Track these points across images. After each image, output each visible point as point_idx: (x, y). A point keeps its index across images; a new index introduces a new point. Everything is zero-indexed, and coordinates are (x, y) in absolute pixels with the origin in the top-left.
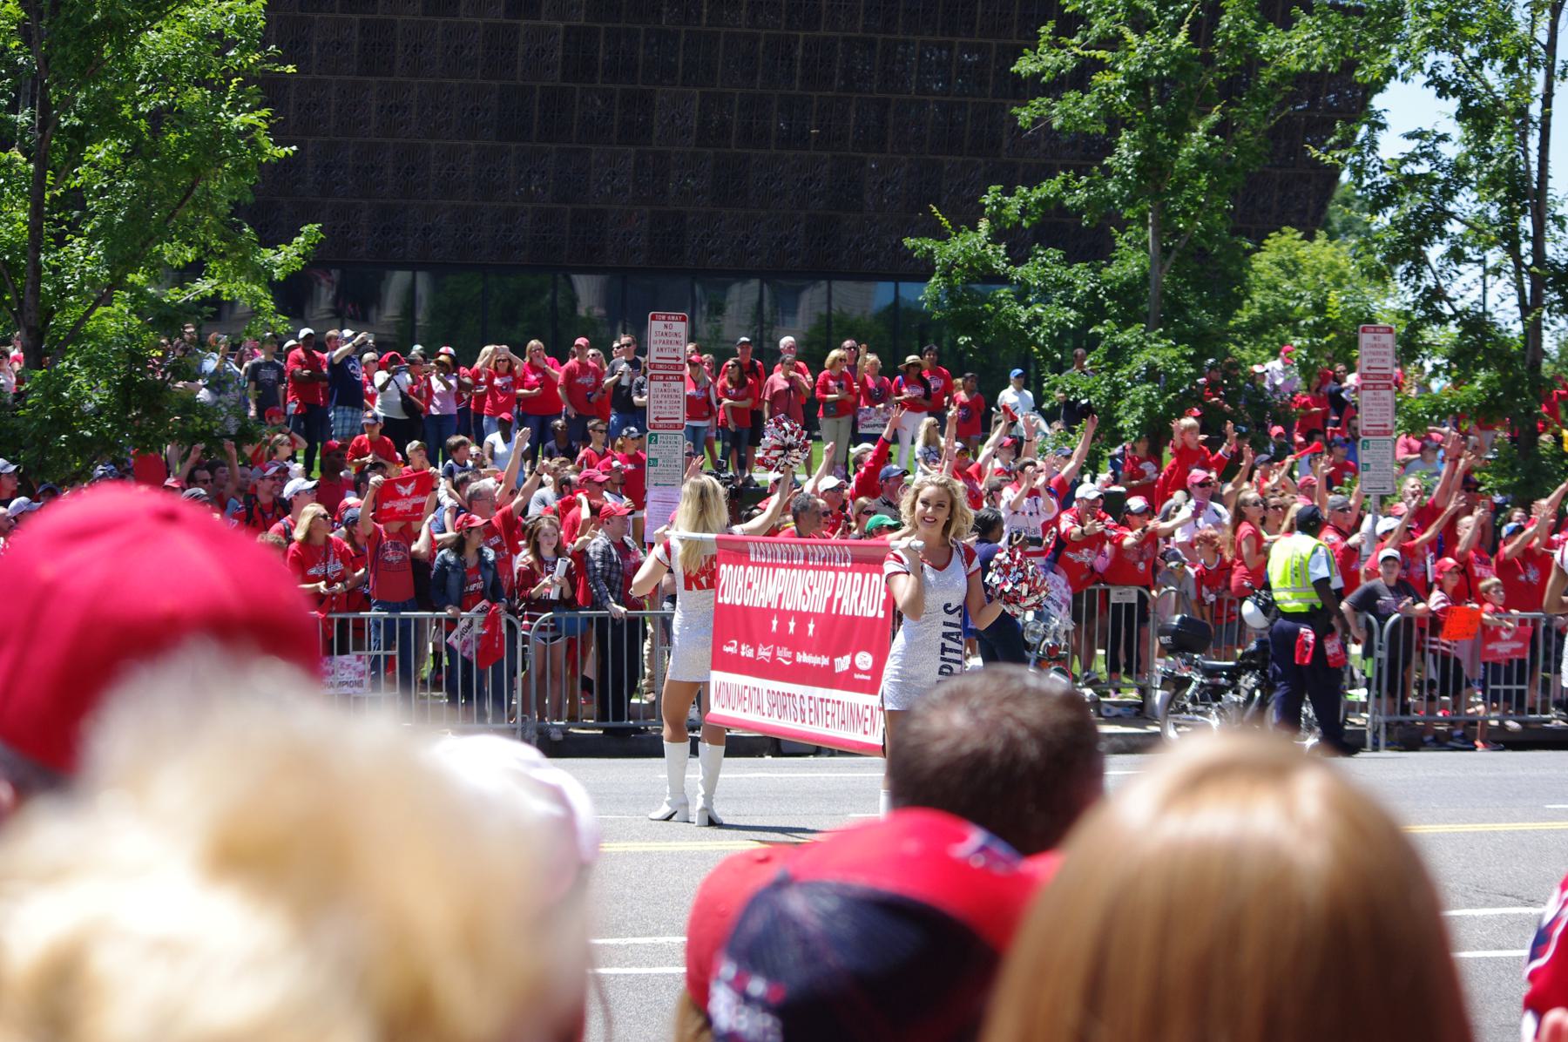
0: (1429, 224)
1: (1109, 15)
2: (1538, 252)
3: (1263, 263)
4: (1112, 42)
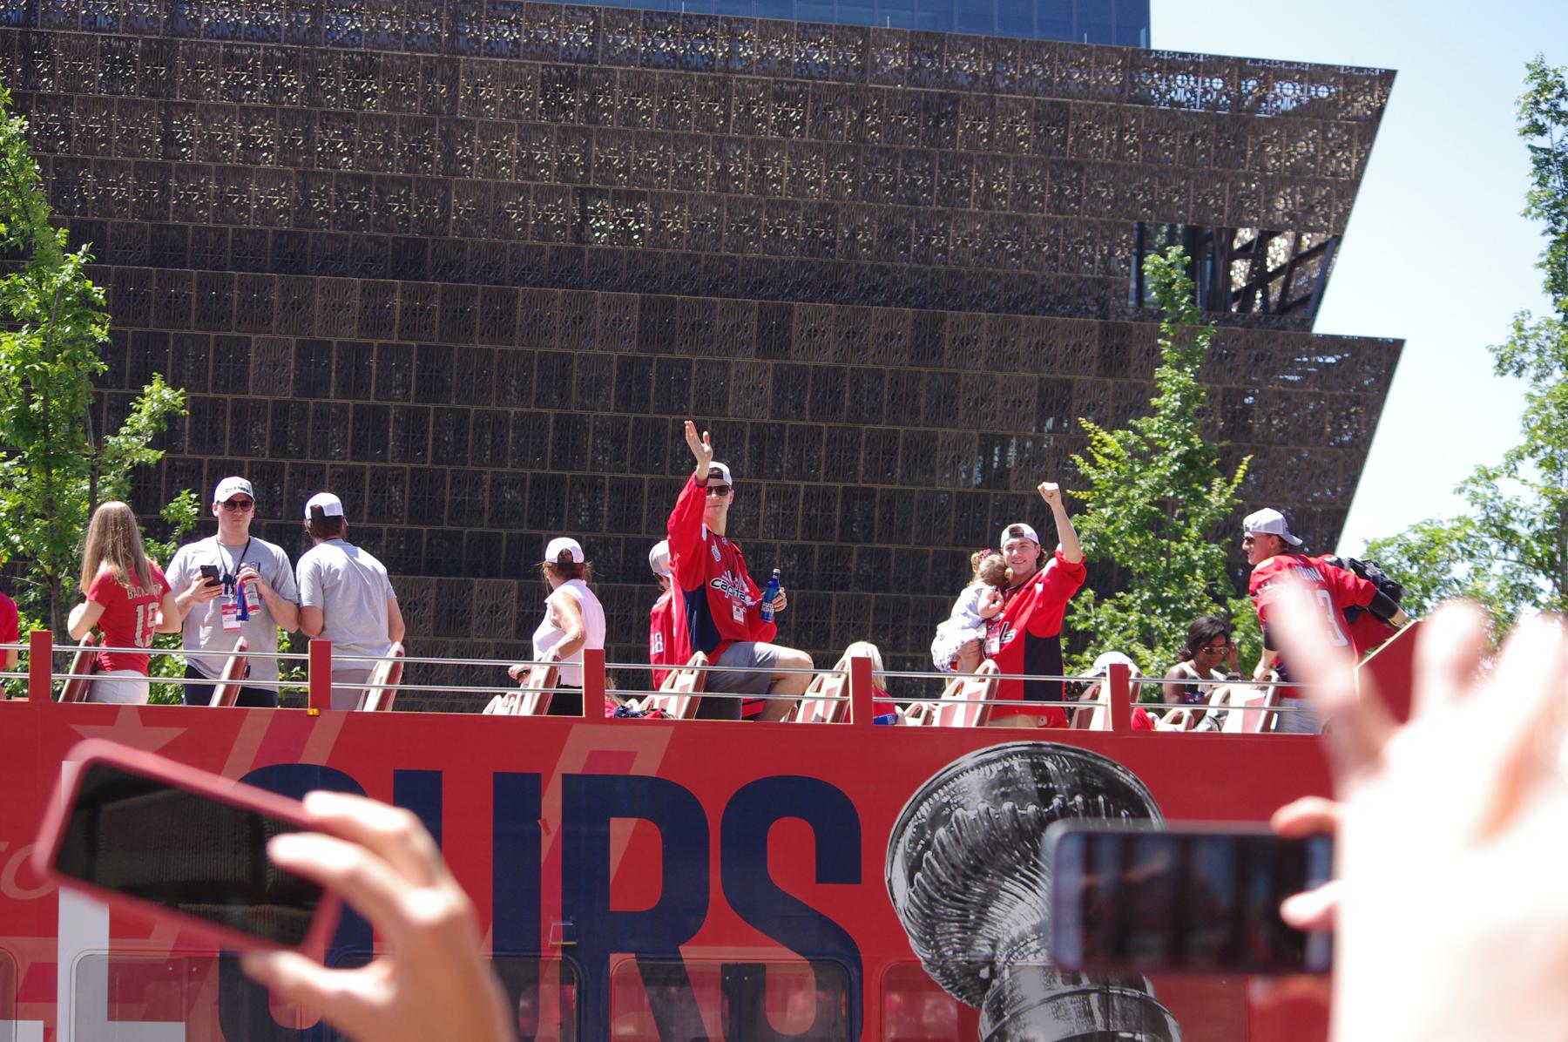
1: (1120, 633)
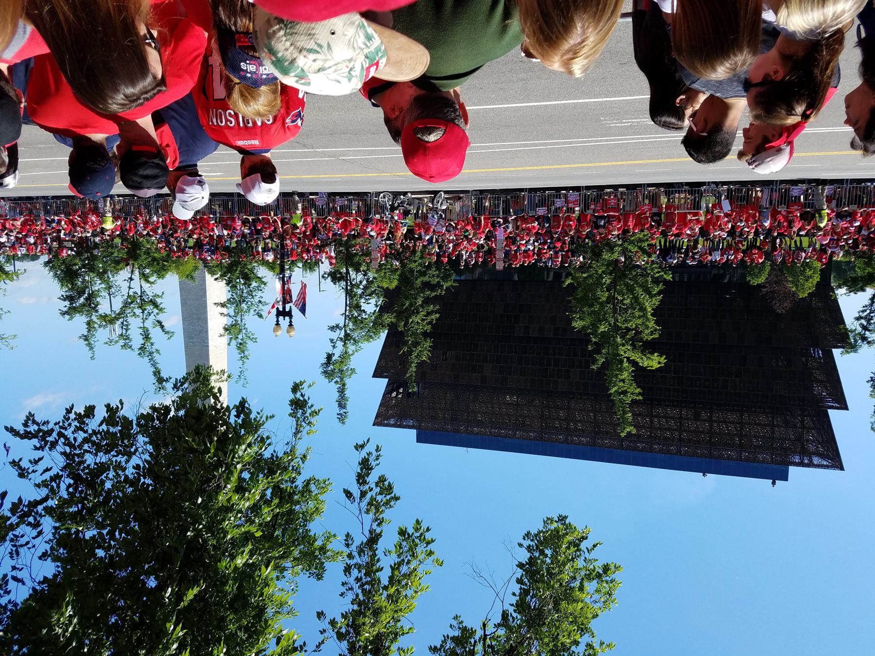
0: (366, 288)
2: (347, 283)
3: (395, 283)
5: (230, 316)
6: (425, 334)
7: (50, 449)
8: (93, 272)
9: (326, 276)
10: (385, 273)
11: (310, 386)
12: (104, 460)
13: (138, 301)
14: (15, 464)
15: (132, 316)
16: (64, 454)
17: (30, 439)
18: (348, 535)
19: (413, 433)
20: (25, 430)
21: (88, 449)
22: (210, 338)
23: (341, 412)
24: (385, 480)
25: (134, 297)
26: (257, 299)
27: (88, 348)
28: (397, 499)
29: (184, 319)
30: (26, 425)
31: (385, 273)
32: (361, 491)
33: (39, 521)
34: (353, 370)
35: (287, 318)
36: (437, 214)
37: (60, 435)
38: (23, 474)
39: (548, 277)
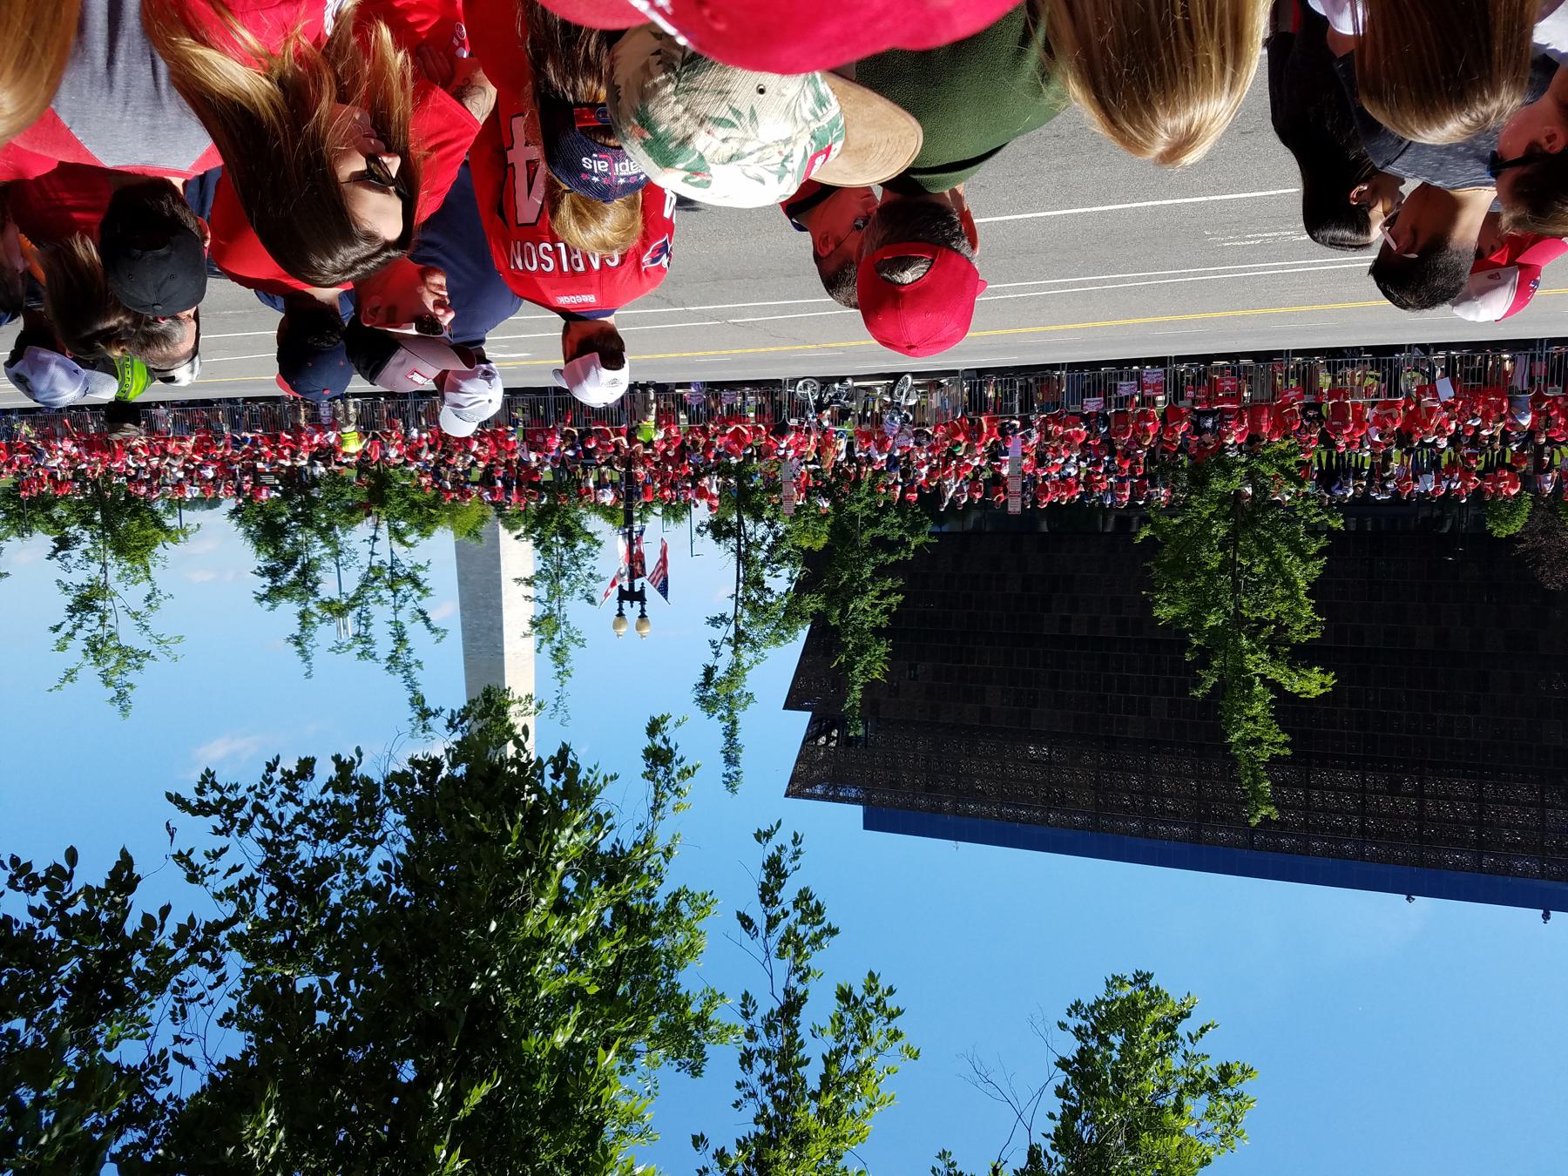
0: (772, 549)
2: (739, 541)
3: (823, 540)
4: (873, 606)
5: (540, 601)
6: (877, 632)
7: (240, 834)
8: (311, 527)
9: (704, 528)
10: (806, 522)
11: (678, 724)
12: (328, 854)
13: (387, 576)
14: (182, 858)
15: (375, 602)
16: (262, 841)
17: (207, 815)
18: (746, 996)
19: (857, 811)
20: (199, 800)
21: (303, 834)
22: (506, 639)
23: (730, 771)
24: (811, 898)
25: (380, 568)
26: (585, 571)
27: (301, 658)
28: (833, 932)
29: (463, 607)
30: (200, 791)
31: (806, 522)
32: (768, 917)
33: (220, 959)
34: (750, 696)
35: (637, 604)
36: (900, 414)
37: (257, 808)
38: (195, 875)
39: (1104, 525)
